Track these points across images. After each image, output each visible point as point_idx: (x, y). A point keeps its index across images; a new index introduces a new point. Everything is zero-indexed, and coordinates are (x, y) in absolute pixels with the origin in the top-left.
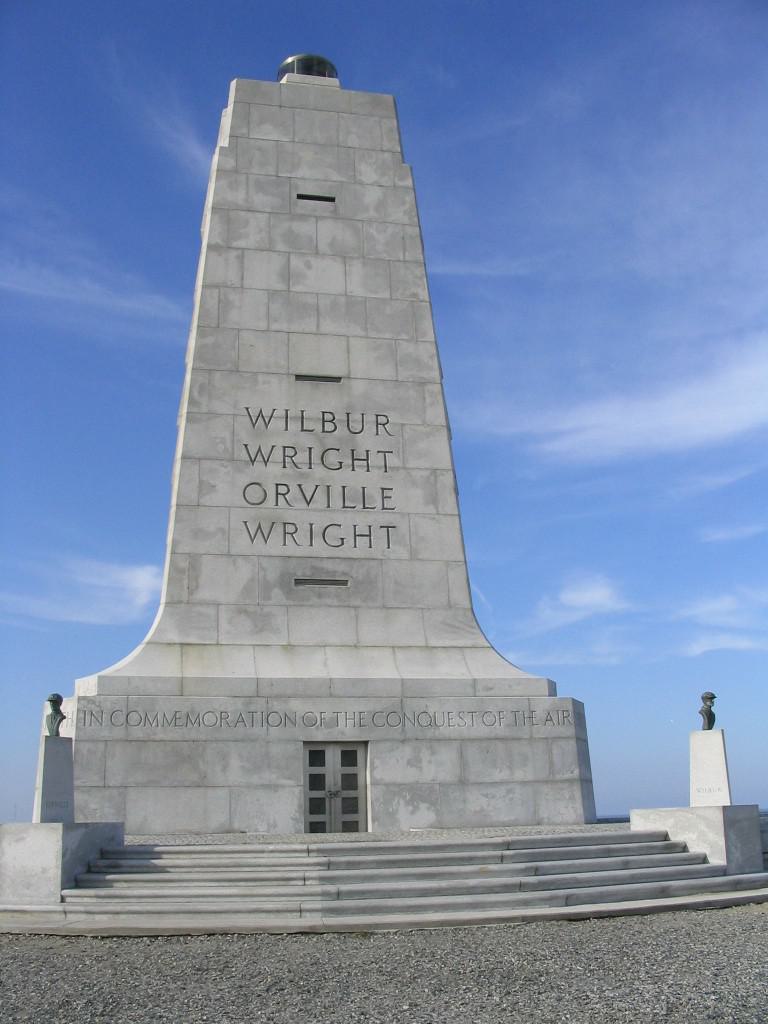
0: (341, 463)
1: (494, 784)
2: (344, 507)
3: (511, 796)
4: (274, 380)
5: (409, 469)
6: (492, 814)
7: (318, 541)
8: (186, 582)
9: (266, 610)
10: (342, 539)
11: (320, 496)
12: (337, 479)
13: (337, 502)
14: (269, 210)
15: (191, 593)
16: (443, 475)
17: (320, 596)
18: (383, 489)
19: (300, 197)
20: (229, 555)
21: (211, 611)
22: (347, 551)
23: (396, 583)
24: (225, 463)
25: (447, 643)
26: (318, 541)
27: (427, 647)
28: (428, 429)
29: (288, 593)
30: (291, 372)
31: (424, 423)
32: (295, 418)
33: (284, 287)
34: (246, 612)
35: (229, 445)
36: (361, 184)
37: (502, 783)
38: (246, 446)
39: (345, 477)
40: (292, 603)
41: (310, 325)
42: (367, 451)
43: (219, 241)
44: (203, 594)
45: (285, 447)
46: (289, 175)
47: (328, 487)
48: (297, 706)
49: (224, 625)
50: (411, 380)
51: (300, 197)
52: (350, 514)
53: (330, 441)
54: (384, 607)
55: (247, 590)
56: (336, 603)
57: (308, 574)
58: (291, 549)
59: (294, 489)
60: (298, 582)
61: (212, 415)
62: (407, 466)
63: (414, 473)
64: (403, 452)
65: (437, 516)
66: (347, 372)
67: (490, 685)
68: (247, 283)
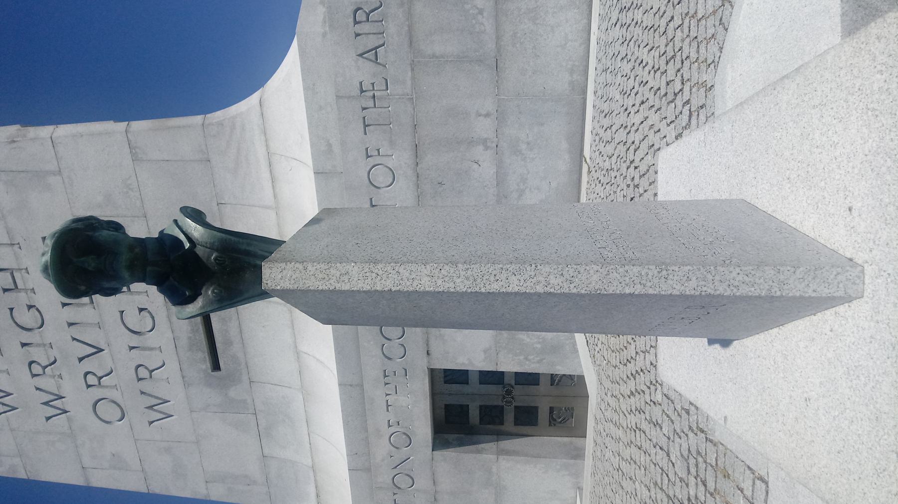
0: (30, 307)
1: (500, 179)
3: (523, 147)
6: (554, 185)
7: (151, 339)
11: (91, 336)
17: (229, 343)
25: (266, 175)
37: (500, 165)
40: (245, 378)
48: (381, 449)
57: (203, 354)
59: (87, 365)
60: (216, 366)
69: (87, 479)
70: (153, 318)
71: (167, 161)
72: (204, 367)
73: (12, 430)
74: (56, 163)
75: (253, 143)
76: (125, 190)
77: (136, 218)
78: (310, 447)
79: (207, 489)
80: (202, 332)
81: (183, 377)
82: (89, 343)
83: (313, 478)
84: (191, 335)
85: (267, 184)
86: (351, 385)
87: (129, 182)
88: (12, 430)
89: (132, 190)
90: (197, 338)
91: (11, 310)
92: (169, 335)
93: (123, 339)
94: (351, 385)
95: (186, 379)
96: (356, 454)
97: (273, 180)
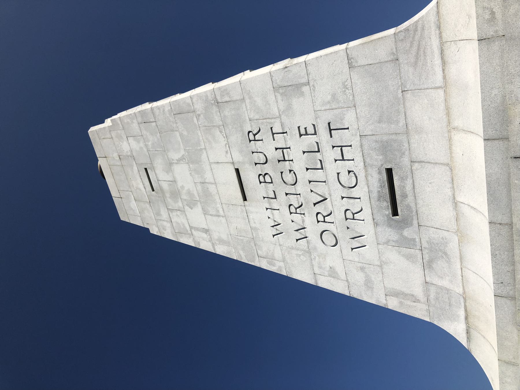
2: (322, 168)
4: (251, 217)
5: (279, 112)
7: (355, 192)
8: (409, 303)
9: (425, 245)
10: (349, 172)
11: (321, 189)
12: (303, 176)
13: (319, 175)
14: (167, 211)
15: (418, 301)
16: (276, 80)
17: (405, 196)
18: (301, 135)
19: (153, 190)
20: (381, 266)
21: (433, 290)
22: (358, 166)
23: (380, 121)
24: (313, 257)
25: (438, 61)
26: (355, 192)
27: (445, 86)
28: (246, 97)
29: (406, 223)
30: (243, 205)
31: (243, 100)
32: (270, 203)
33: (199, 204)
34: (431, 262)
35: (299, 253)
36: (131, 151)
38: (297, 240)
39: (300, 165)
40: (415, 222)
41: (212, 189)
42: (276, 149)
43: (192, 239)
44: (418, 291)
45: (291, 213)
46: (146, 196)
47: (310, 182)
49: (445, 283)
50: (219, 114)
51: (153, 190)
52: (326, 165)
53: (277, 179)
54: (407, 133)
55: (409, 257)
56: (409, 182)
57: (387, 204)
58: (366, 214)
59: (319, 208)
60: (395, 213)
61: (284, 260)
62: (277, 114)
63: (282, 108)
64: (269, 118)
65: (311, 83)
66: (230, 164)
67: (487, 17)
68: (206, 227)
69: (316, 281)
70: (356, 177)
71: (370, 64)
72: (387, 213)
73: (280, 245)
74: (307, 78)
75: (430, 38)
76: (344, 90)
77: (349, 108)
78: (462, 279)
79: (386, 300)
80: (387, 187)
81: (374, 219)
82: (320, 193)
83: (463, 304)
84: (380, 190)
85: (438, 70)
86: (500, 224)
87: (346, 83)
88: (280, 245)
89: (347, 88)
90: (384, 191)
91: (282, 173)
92: (366, 189)
93: (338, 191)
94: (500, 224)
95: (375, 221)
96: (502, 283)
97: (444, 63)
